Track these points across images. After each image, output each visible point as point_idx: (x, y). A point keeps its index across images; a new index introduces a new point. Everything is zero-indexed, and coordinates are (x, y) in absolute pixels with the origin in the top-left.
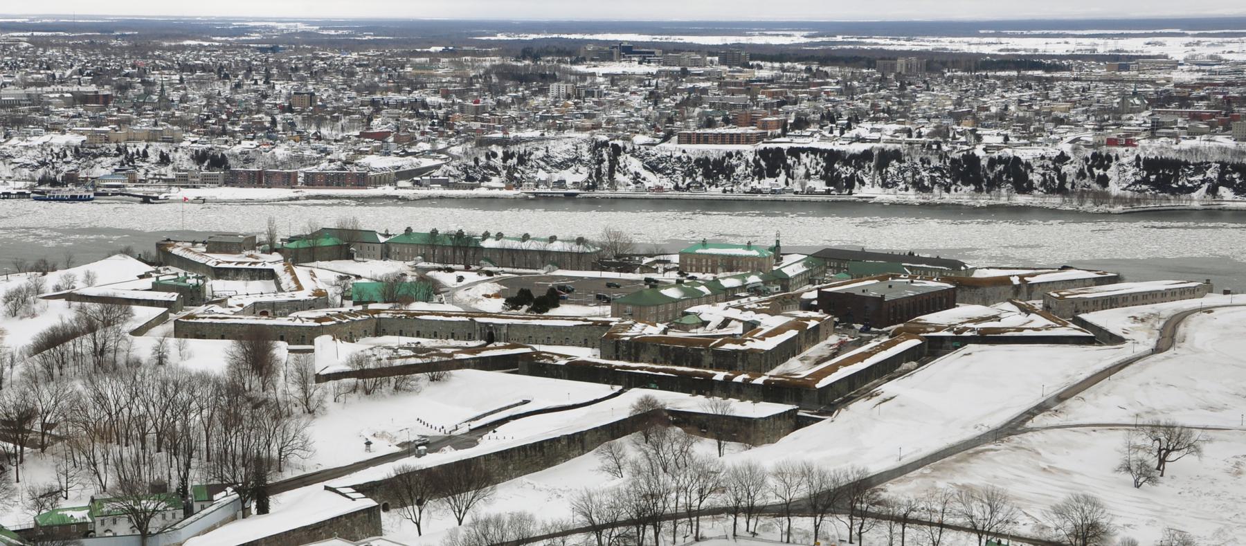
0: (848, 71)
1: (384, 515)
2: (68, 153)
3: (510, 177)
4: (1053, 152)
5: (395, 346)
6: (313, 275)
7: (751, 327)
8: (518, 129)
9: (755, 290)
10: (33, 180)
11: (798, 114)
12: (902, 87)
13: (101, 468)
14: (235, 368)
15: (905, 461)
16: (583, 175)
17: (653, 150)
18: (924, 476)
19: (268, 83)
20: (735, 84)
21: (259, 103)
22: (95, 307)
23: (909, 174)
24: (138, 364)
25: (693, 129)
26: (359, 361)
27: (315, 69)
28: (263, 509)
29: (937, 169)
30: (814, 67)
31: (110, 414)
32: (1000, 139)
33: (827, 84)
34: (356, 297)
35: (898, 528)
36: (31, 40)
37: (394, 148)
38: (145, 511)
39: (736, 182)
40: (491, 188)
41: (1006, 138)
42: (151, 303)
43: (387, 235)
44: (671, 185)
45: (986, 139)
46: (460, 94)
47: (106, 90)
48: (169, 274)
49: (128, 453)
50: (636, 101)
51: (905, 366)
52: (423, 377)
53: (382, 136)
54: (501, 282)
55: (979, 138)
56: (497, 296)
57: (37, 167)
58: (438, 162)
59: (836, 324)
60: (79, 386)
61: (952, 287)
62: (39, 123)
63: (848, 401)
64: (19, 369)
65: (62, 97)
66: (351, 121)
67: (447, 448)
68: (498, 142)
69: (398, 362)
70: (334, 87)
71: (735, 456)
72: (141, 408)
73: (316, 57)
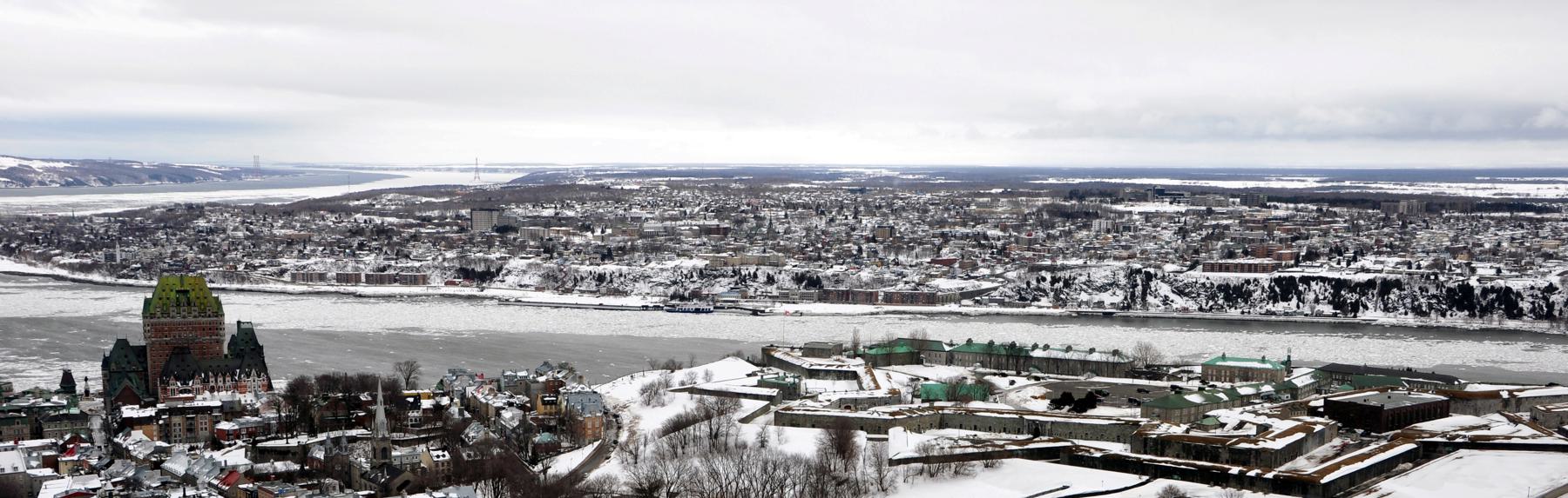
0: (1355, 211)
2: (694, 274)
3: (1057, 298)
4: (1542, 283)
5: (955, 437)
6: (889, 377)
7: (1263, 429)
8: (1065, 258)
9: (1268, 398)
10: (666, 296)
11: (1309, 247)
12: (1404, 226)
14: (823, 452)
16: (1119, 297)
17: (1180, 277)
19: (857, 218)
20: (1254, 222)
21: (848, 234)
22: (712, 399)
23: (1409, 300)
24: (744, 446)
25: (1216, 259)
26: (926, 449)
27: (896, 207)
29: (1434, 296)
30: (1325, 209)
31: (721, 486)
32: (1493, 272)
33: (1336, 222)
34: (924, 396)
36: (669, 184)
37: (959, 272)
39: (1253, 305)
40: (1040, 307)
41: (1499, 271)
42: (756, 397)
43: (951, 345)
45: (1480, 272)
46: (1016, 228)
47: (726, 224)
48: (771, 374)
50: (1167, 235)
51: (1402, 466)
52: (979, 464)
53: (949, 263)
54: (1046, 386)
55: (1473, 270)
56: (1043, 397)
57: (670, 286)
58: (995, 285)
59: (1340, 428)
60: (696, 462)
61: (1446, 398)
62: (673, 250)
64: (651, 447)
65: (691, 229)
66: (924, 250)
68: (1047, 268)
69: (958, 451)
70: (911, 222)
72: (746, 482)
73: (896, 197)
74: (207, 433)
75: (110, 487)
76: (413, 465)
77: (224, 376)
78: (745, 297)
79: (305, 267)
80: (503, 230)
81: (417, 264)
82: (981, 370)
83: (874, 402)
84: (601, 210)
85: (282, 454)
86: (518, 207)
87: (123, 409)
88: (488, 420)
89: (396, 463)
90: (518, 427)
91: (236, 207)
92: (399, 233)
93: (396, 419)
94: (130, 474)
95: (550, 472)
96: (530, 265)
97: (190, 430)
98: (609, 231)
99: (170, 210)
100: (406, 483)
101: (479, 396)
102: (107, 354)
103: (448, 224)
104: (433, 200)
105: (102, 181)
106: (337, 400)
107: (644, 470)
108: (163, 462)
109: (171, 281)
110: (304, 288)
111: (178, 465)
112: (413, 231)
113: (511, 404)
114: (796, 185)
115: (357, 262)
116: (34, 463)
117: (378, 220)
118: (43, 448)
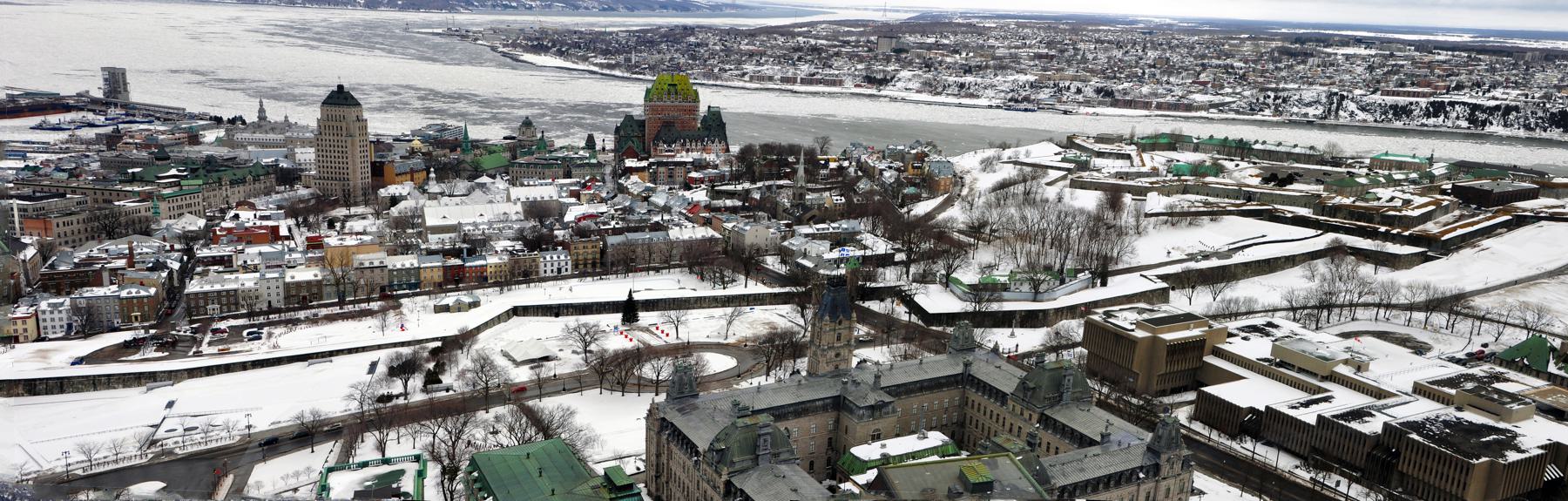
0: (1494, 58)
1: (1171, 292)
3: (1276, 110)
7: (1407, 203)
8: (1285, 83)
9: (1413, 182)
12: (1527, 69)
14: (1101, 207)
15: (1489, 285)
16: (1320, 111)
17: (1365, 99)
18: (1499, 294)
21: (1137, 62)
22: (1028, 169)
24: (1047, 201)
25: (1392, 87)
26: (1171, 207)
28: (1104, 284)
29: (1541, 118)
35: (1477, 323)
37: (1210, 90)
39: (1413, 120)
43: (1198, 139)
44: (1372, 119)
46: (1255, 62)
47: (1053, 52)
48: (1072, 153)
49: (1034, 248)
50: (1359, 70)
51: (1499, 231)
53: (1204, 84)
56: (1257, 176)
60: (1013, 210)
62: (1014, 69)
63: (1459, 248)
64: (983, 199)
67: (1214, 259)
69: (1193, 209)
71: (1385, 275)
74: (682, 179)
75: (613, 212)
76: (819, 205)
77: (696, 142)
78: (1060, 101)
80: (898, 51)
81: (837, 72)
82: (1217, 156)
83: (1140, 175)
85: (731, 195)
87: (626, 161)
92: (827, 51)
93: (811, 175)
94: (627, 204)
95: (912, 213)
96: (914, 76)
98: (971, 54)
100: (814, 216)
101: (870, 161)
104: (853, 29)
105: (628, 9)
106: (773, 160)
107: (976, 214)
111: (659, 199)
112: (836, 50)
114: (1105, 28)
116: (564, 194)
117: (813, 42)
118: (571, 185)
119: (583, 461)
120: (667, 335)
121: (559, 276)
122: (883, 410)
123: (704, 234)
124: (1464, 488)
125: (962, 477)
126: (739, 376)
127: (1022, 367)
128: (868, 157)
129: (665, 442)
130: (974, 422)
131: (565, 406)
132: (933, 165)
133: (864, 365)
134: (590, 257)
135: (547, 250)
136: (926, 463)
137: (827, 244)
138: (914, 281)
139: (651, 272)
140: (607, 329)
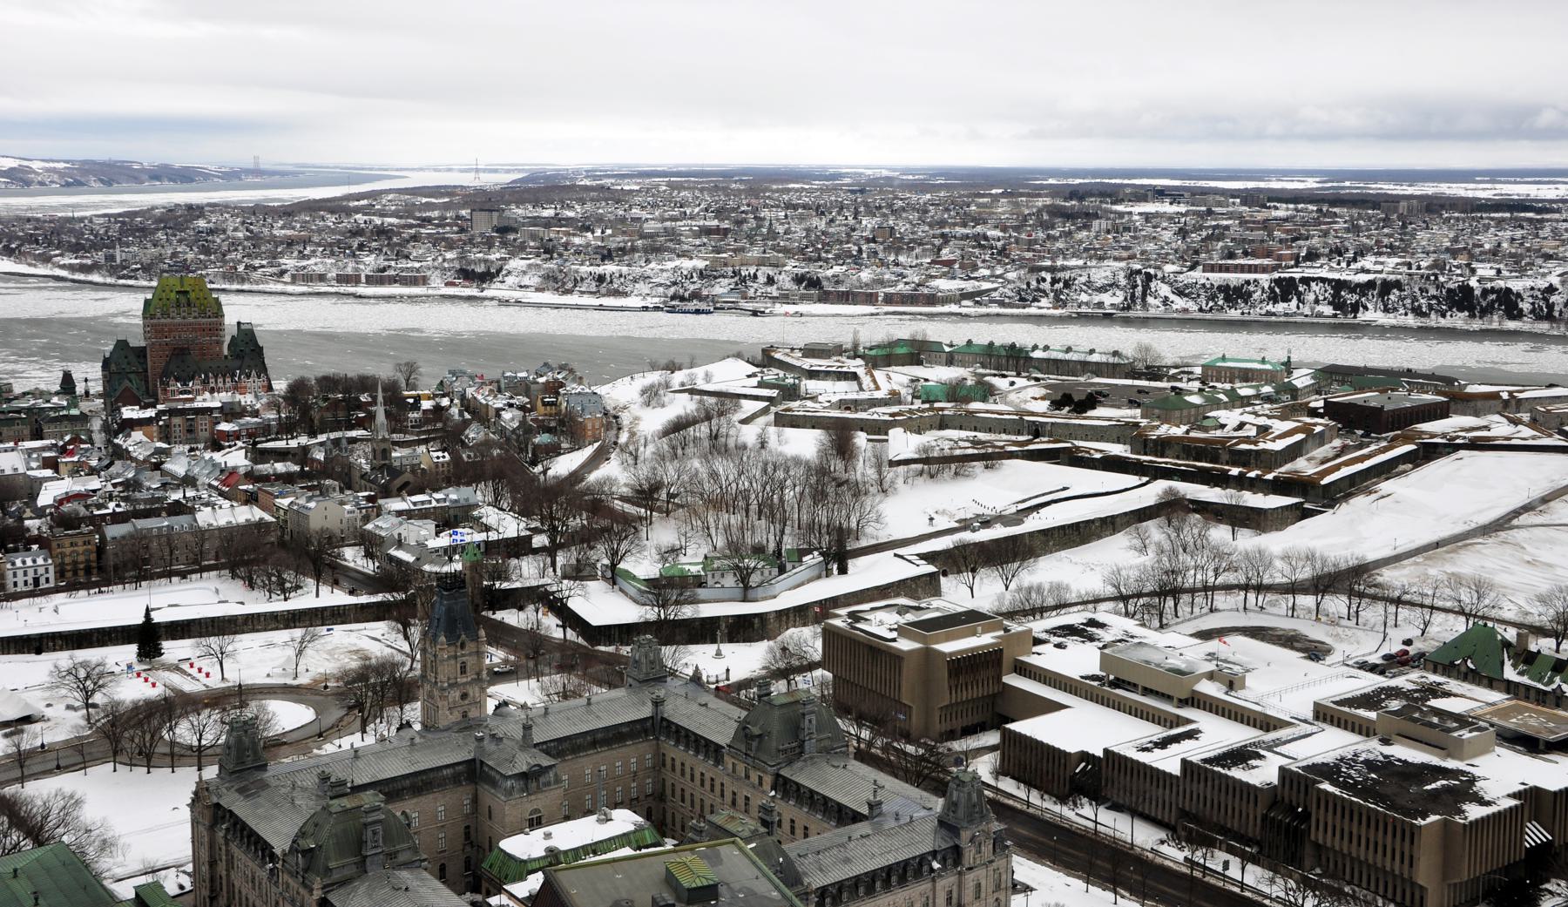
0: (1355, 212)
1: (943, 579)
3: (1057, 299)
4: (1542, 284)
5: (955, 438)
6: (889, 378)
7: (1263, 430)
8: (1065, 258)
9: (1268, 399)
11: (1309, 248)
12: (1404, 226)
13: (713, 531)
14: (823, 453)
15: (1400, 550)
16: (1119, 298)
17: (1181, 278)
18: (1416, 564)
20: (1254, 222)
21: (848, 235)
22: (712, 400)
23: (1409, 301)
24: (744, 447)
25: (1216, 260)
26: (926, 450)
27: (896, 207)
28: (843, 570)
29: (1434, 297)
30: (1324, 209)
32: (1493, 272)
33: (1336, 223)
34: (924, 397)
35: (1392, 609)
36: (669, 184)
37: (959, 273)
38: (748, 568)
39: (1253, 306)
40: (1040, 308)
41: (1499, 271)
42: (756, 398)
43: (951, 346)
44: (1196, 308)
45: (1480, 272)
46: (1016, 229)
47: (726, 225)
48: (771, 374)
49: (735, 520)
50: (1167, 235)
51: (1401, 467)
52: (979, 465)
53: (949, 263)
54: (1046, 387)
55: (1473, 271)
56: (1043, 398)
58: (995, 285)
59: (1340, 429)
60: (696, 463)
62: (673, 251)
63: (1348, 496)
64: (651, 448)
65: (691, 230)
66: (924, 250)
67: (998, 525)
68: (1047, 269)
69: (958, 452)
70: (911, 223)
71: (1247, 541)
73: (896, 198)
74: (207, 434)
75: (110, 488)
76: (413, 466)
77: (224, 376)
78: (745, 297)
79: (305, 268)
80: (503, 230)
81: (417, 265)
82: (981, 371)
83: (874, 403)
84: (601, 211)
85: (282, 455)
86: (518, 207)
87: (123, 410)
88: (489, 421)
89: (397, 464)
90: (518, 428)
91: (236, 208)
92: (399, 234)
93: (396, 421)
94: (130, 475)
95: (550, 473)
96: (530, 266)
97: (190, 431)
98: (609, 232)
99: (170, 211)
100: (406, 484)
101: (479, 397)
102: (107, 355)
103: (448, 225)
104: (433, 200)
105: (102, 181)
107: (644, 471)
108: (163, 463)
109: (171, 282)
110: (304, 289)
112: (413, 231)
113: (511, 405)
114: (796, 186)
115: (357, 263)
116: (34, 465)
117: (378, 221)
118: (43, 449)
119: (97, 878)
120: (208, 675)
121: (36, 590)
122: (542, 780)
123: (249, 517)
124: (1411, 865)
125: (670, 880)
126: (320, 735)
127: (737, 703)
128: (477, 391)
129: (222, 841)
130: (678, 792)
131: (68, 790)
132: (571, 399)
133: (504, 709)
134: (81, 558)
135: (16, 550)
136: (614, 860)
137: (430, 525)
138: (565, 577)
139: (175, 579)
140: (117, 670)
